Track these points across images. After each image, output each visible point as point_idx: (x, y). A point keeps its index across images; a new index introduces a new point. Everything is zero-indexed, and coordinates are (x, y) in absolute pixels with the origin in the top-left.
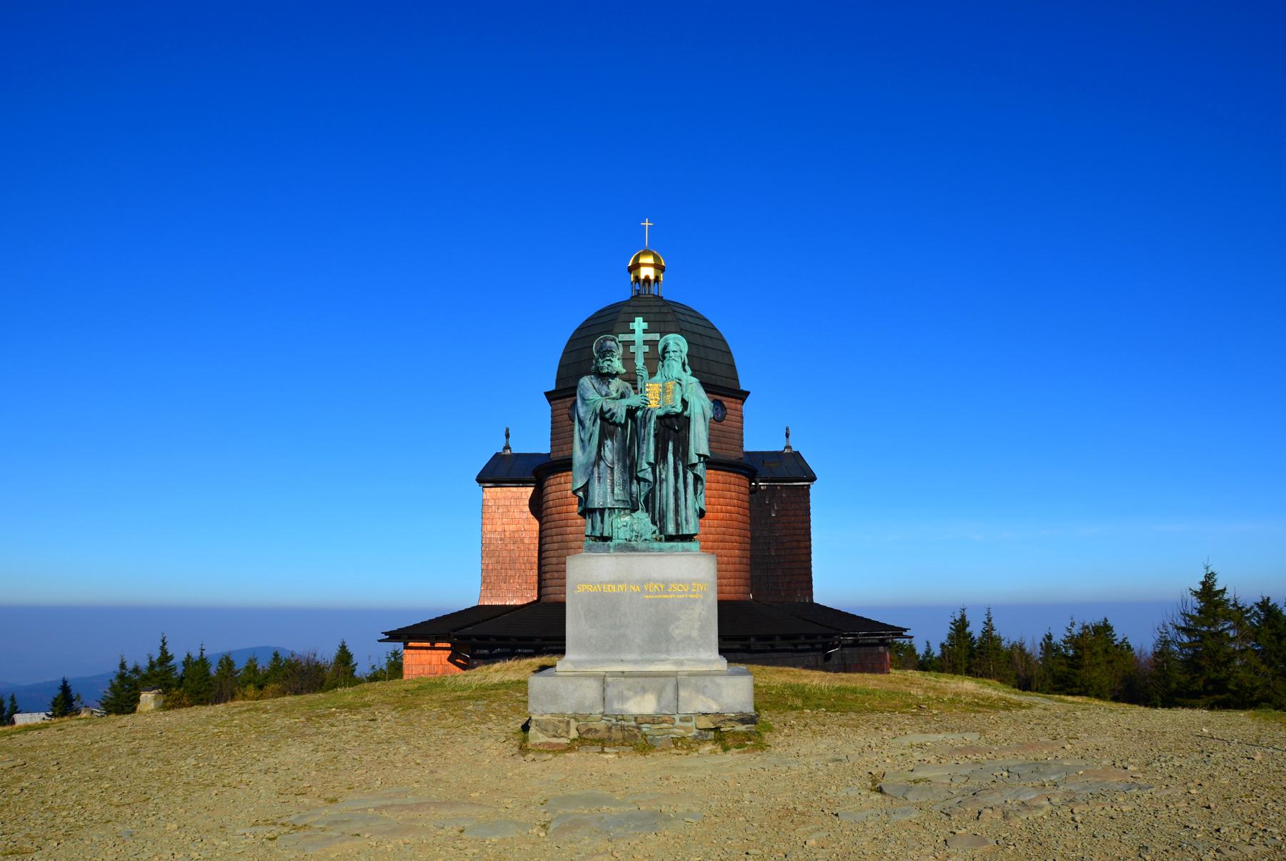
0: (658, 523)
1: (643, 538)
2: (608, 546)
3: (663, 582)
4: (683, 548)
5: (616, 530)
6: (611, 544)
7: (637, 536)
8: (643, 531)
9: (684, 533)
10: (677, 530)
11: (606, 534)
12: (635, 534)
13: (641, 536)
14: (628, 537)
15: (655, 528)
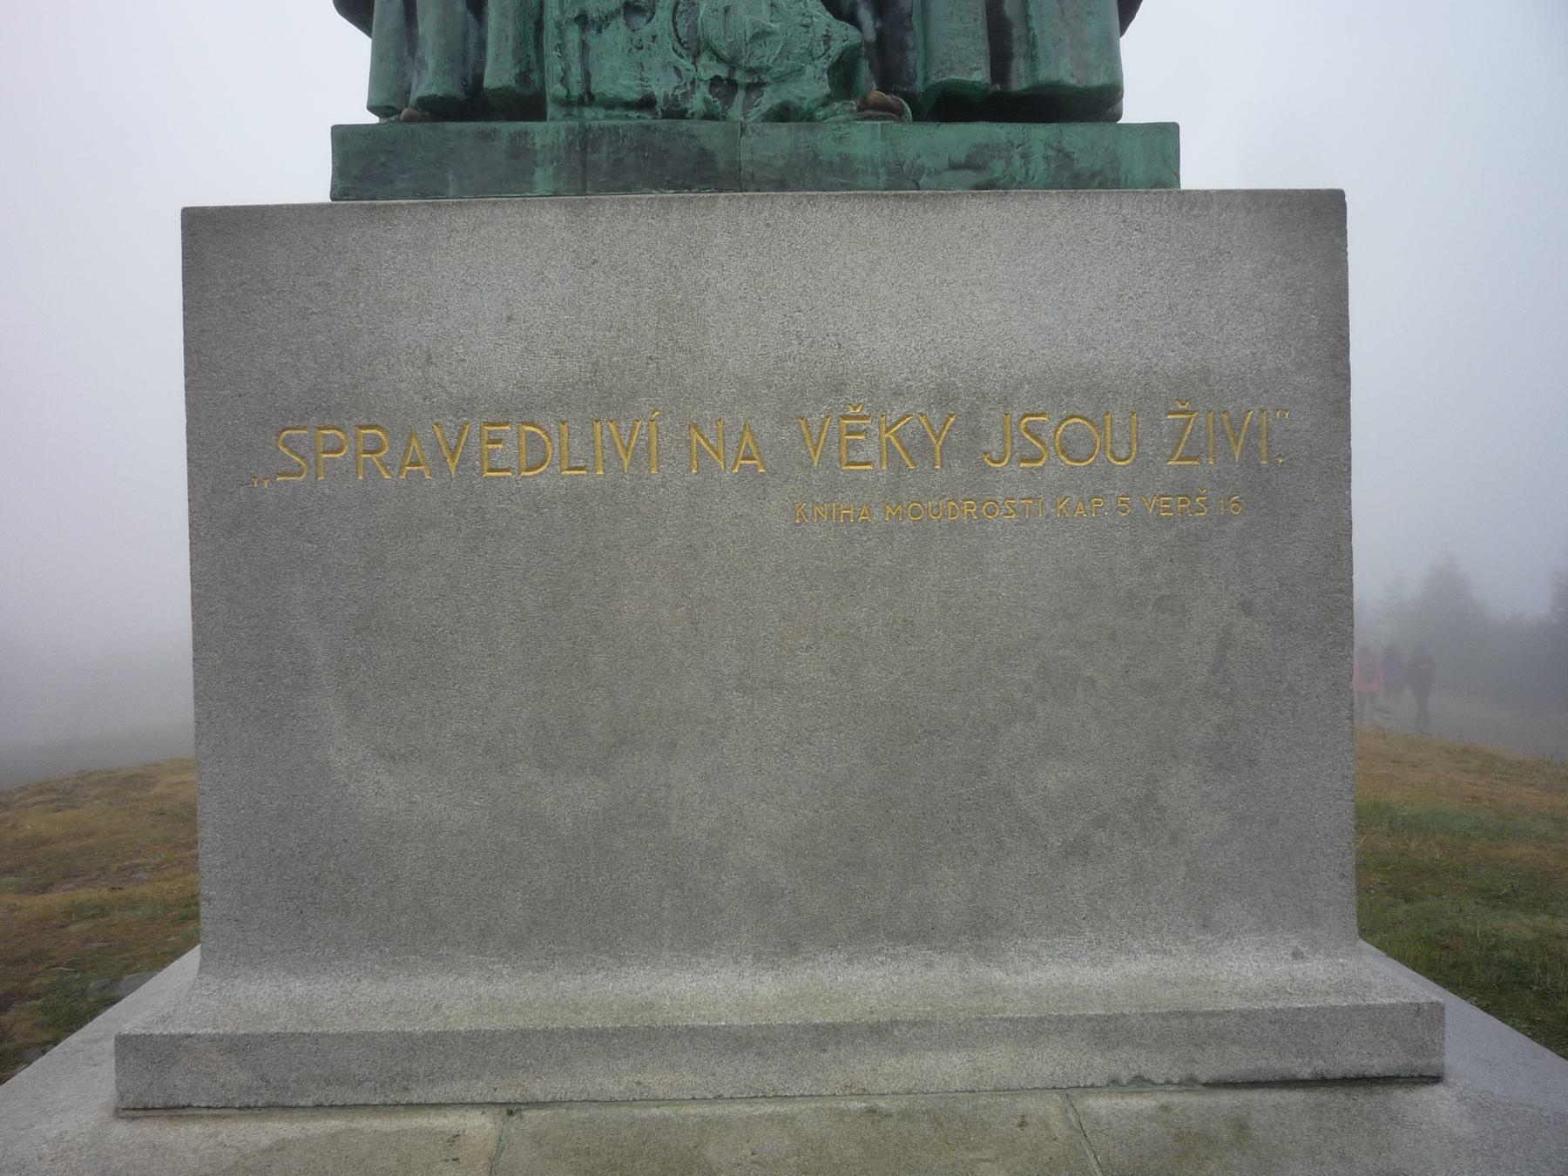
0: (865, 15)
1: (769, 99)
2: (520, 151)
3: (944, 397)
4: (1065, 157)
5: (573, 35)
6: (546, 133)
7: (724, 87)
8: (767, 54)
9: (1046, 74)
10: (1000, 60)
11: (498, 74)
12: (709, 69)
13: (755, 87)
14: (662, 87)
15: (844, 35)
